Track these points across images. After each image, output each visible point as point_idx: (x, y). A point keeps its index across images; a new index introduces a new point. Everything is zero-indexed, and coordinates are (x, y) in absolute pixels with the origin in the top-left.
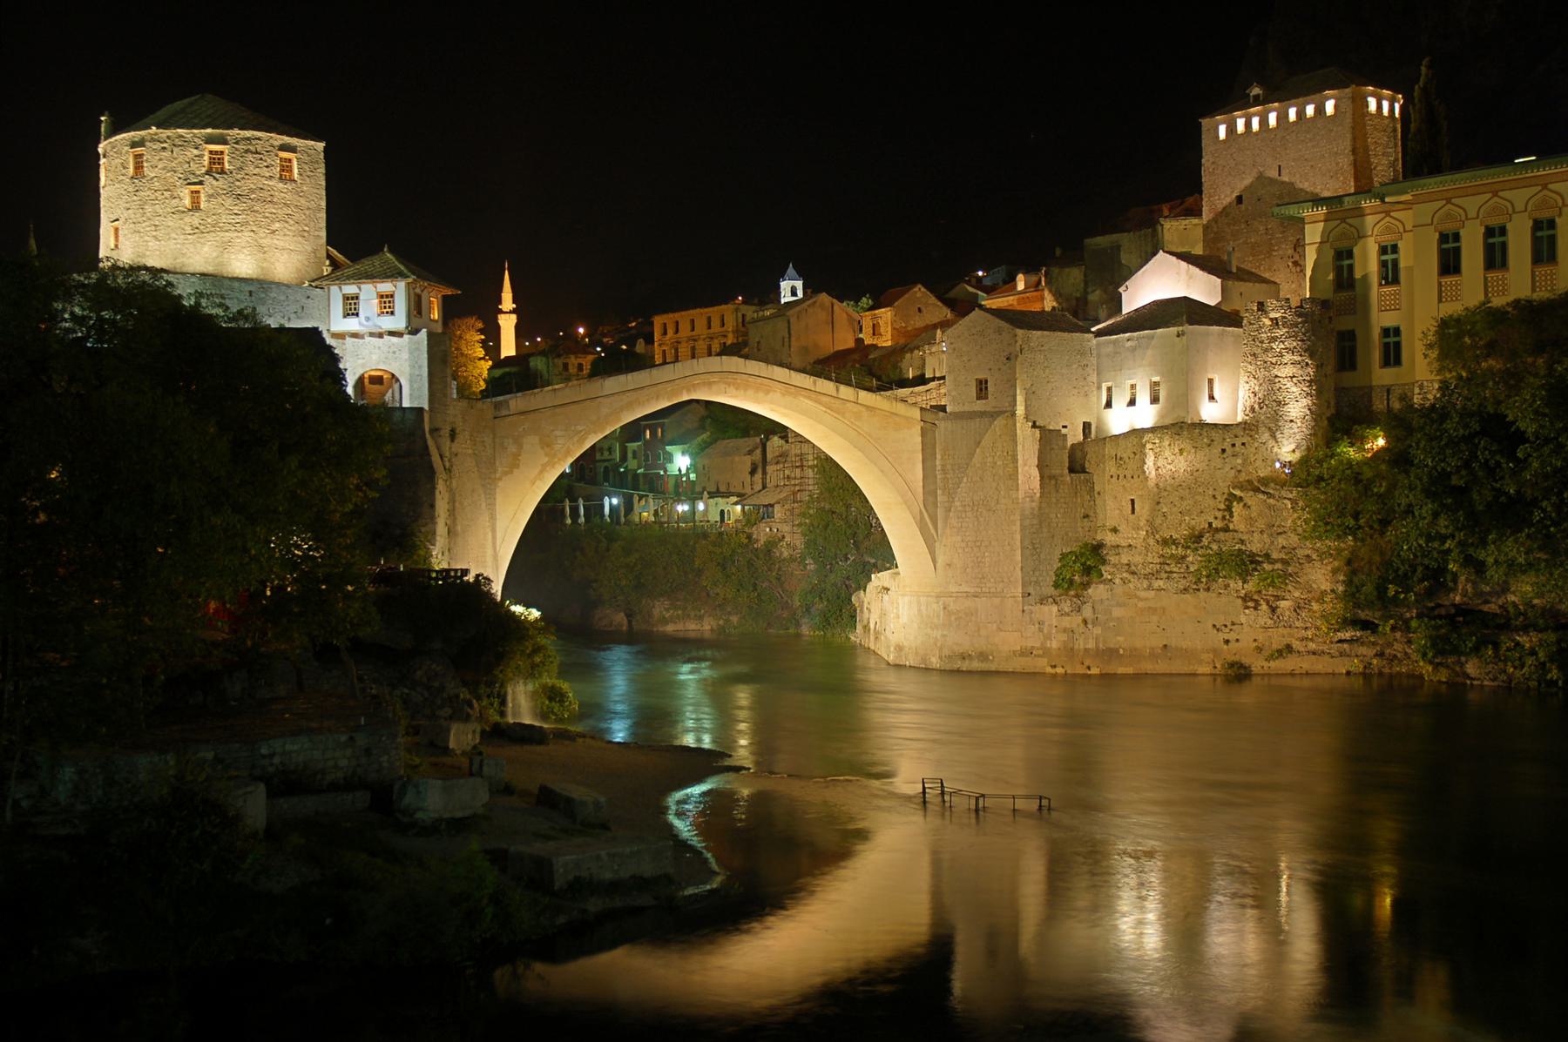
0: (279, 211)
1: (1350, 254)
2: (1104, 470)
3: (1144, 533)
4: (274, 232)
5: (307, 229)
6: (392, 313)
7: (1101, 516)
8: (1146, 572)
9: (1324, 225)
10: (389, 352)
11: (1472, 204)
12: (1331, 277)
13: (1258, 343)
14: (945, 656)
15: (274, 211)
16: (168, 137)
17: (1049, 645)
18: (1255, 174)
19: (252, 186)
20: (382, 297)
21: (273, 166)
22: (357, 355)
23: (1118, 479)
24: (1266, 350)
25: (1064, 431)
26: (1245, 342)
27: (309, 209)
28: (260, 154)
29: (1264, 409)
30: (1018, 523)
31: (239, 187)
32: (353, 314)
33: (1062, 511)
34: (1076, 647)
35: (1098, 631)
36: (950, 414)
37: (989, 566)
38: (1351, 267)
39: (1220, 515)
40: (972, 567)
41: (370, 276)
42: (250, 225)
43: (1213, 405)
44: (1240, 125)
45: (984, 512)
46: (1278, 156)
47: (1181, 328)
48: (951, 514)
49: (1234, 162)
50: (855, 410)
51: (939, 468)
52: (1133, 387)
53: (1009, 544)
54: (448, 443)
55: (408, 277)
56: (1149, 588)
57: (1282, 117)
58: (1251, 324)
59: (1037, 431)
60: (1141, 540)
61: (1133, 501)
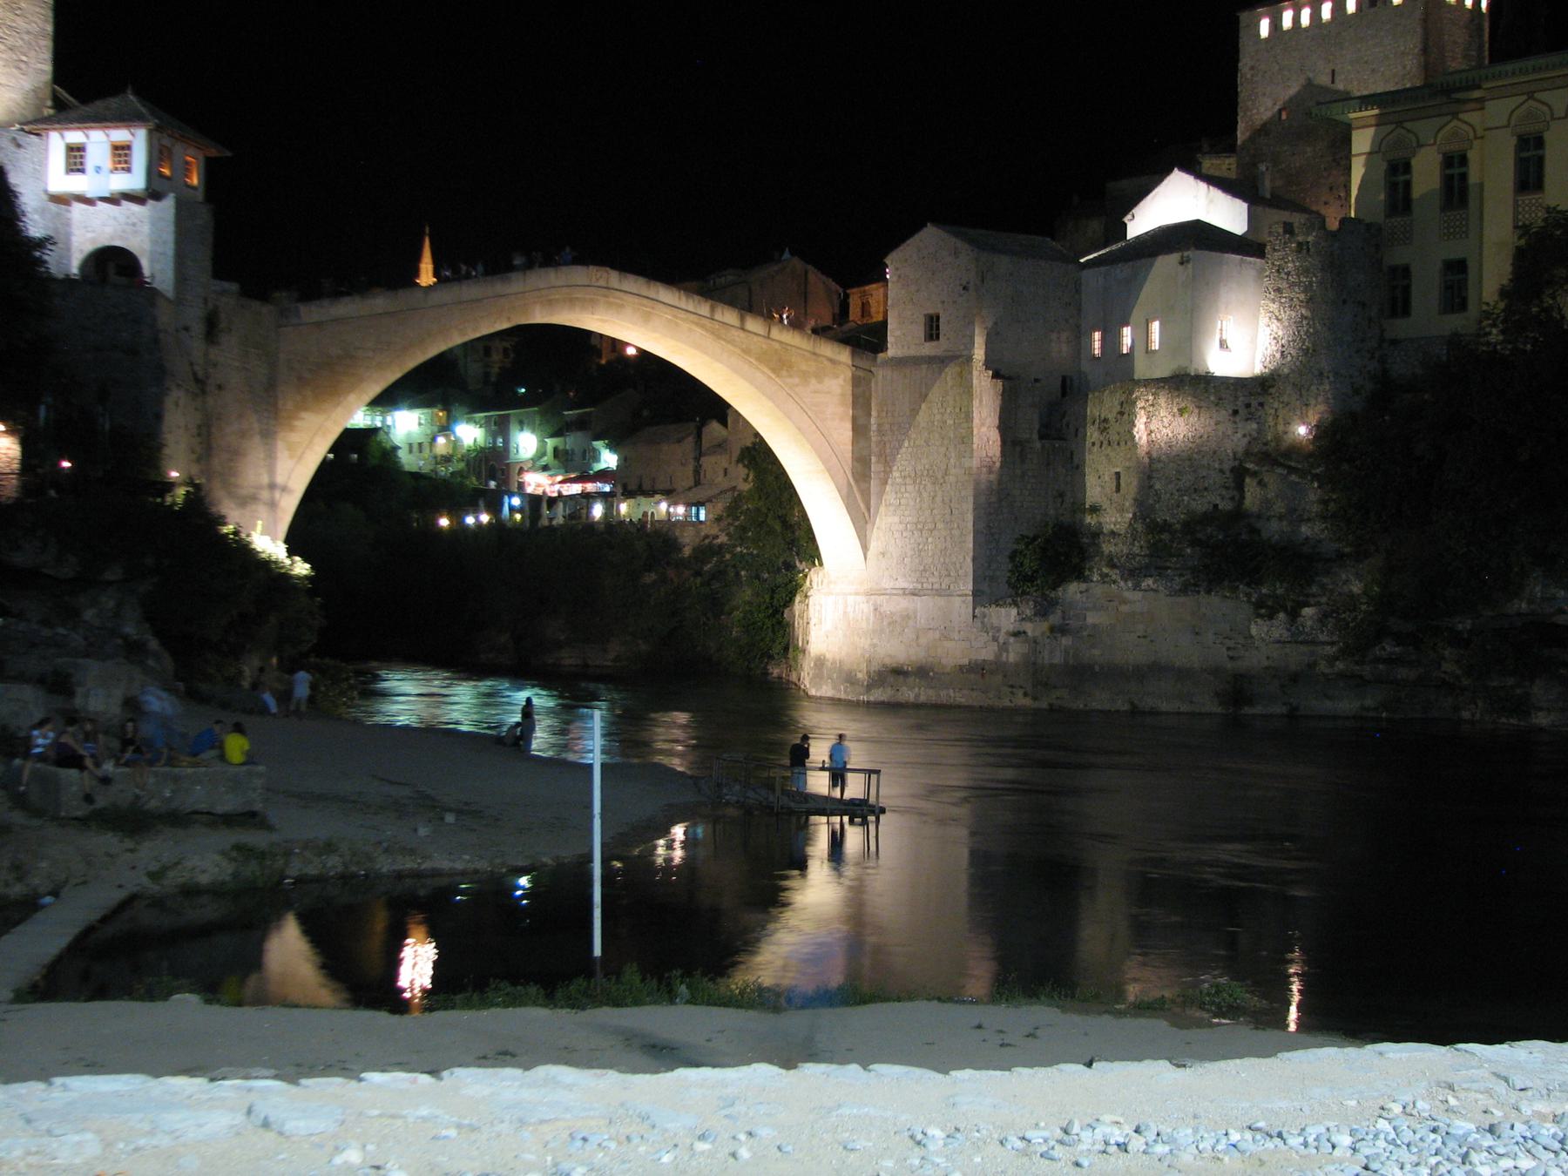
1: (1407, 168)
3: (1131, 515)
5: (24, 58)
9: (1376, 130)
12: (1382, 197)
13: (1283, 275)
14: (874, 671)
18: (1302, 81)
23: (1101, 447)
26: (1267, 273)
27: (28, 33)
30: (971, 499)
32: (79, 170)
33: (1029, 487)
34: (1039, 661)
35: (1066, 641)
37: (933, 555)
38: (1408, 184)
40: (912, 556)
43: (1224, 353)
45: (929, 485)
46: (1331, 57)
48: (888, 488)
49: (1277, 67)
51: (874, 427)
53: (958, 527)
56: (1137, 587)
58: (1275, 250)
61: (1118, 474)
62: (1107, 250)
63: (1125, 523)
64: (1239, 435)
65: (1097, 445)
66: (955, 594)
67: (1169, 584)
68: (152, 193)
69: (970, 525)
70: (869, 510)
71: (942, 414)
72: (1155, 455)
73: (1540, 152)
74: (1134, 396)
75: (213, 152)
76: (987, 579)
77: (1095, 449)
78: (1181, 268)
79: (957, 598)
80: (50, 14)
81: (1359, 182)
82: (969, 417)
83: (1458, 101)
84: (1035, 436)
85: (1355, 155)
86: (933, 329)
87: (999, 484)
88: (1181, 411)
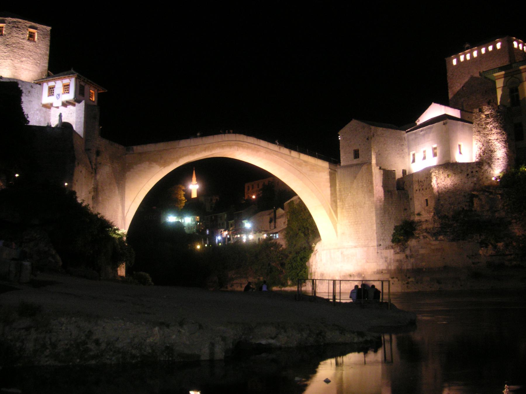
0: (26, 53)
1: (517, 90)
2: (413, 189)
3: (433, 214)
4: (22, 62)
5: (39, 62)
6: (69, 93)
7: (412, 209)
8: (434, 232)
10: (69, 114)
12: (509, 101)
14: (342, 276)
15: (23, 53)
18: (469, 76)
19: (14, 41)
21: (25, 34)
22: (55, 116)
23: (420, 191)
24: (484, 129)
26: (474, 126)
27: (40, 54)
28: (19, 28)
29: (485, 155)
31: (8, 41)
32: (52, 95)
36: (343, 166)
38: (518, 96)
39: (467, 204)
42: (10, 57)
43: (460, 155)
47: (445, 121)
50: (298, 162)
52: (424, 152)
54: (95, 157)
55: (75, 74)
57: (479, 53)
58: (476, 118)
59: (382, 171)
60: (431, 217)
61: (427, 200)
62: (414, 127)
63: (431, 216)
64: (470, 183)
65: (418, 191)
66: (370, 246)
67: (448, 238)
68: (77, 100)
69: (374, 221)
72: (440, 191)
74: (431, 171)
76: (382, 240)
77: (418, 191)
78: (444, 126)
79: (371, 247)
80: (49, 48)
82: (371, 183)
84: (395, 189)
85: (498, 88)
86: (356, 155)
87: (384, 206)
88: (448, 176)
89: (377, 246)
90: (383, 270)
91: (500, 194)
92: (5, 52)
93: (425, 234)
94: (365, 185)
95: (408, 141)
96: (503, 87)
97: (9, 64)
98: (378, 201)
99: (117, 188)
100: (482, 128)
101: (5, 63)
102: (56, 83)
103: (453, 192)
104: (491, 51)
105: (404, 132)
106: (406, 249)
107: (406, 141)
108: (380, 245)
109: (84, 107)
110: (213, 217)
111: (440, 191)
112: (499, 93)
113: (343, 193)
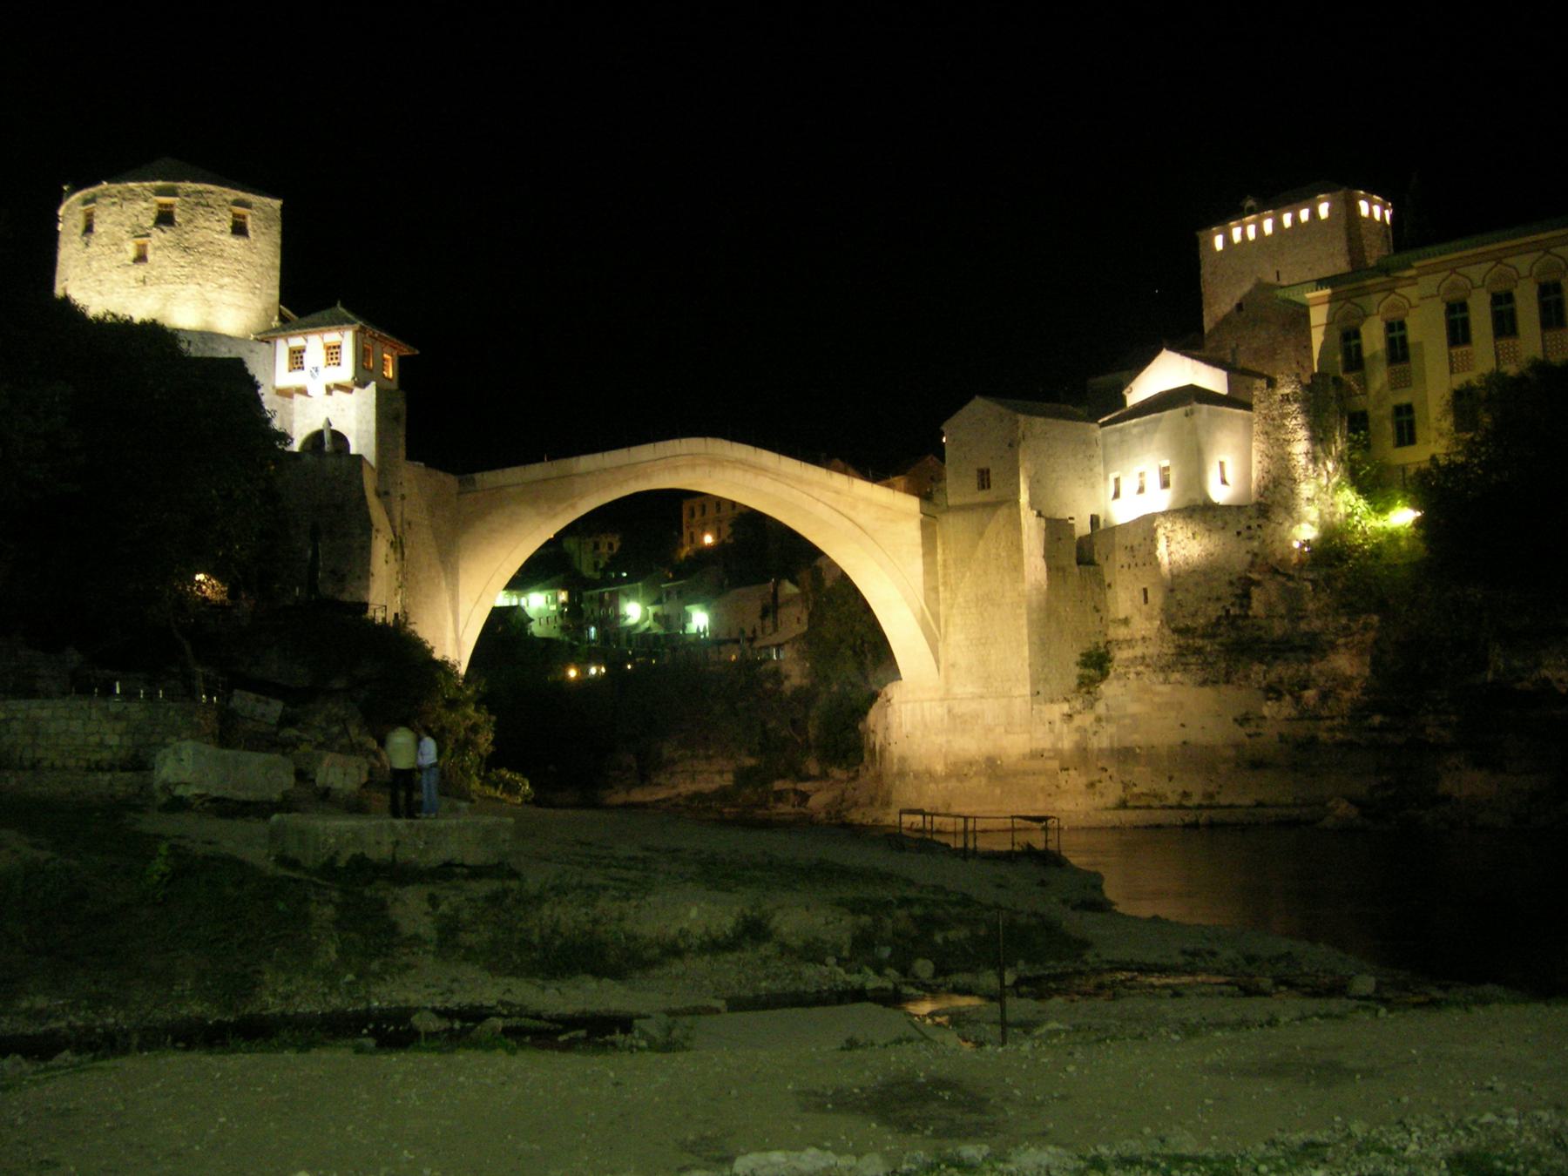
1: (1357, 335)
2: (1115, 560)
3: (1159, 622)
4: (221, 287)
5: (258, 286)
6: (339, 364)
11: (1477, 272)
12: (1339, 358)
13: (1269, 421)
15: (223, 265)
16: (119, 192)
17: (1060, 746)
18: (1253, 280)
20: (329, 348)
25: (1070, 522)
27: (261, 266)
30: (1025, 616)
31: (186, 239)
38: (1359, 348)
41: (316, 326)
44: (1236, 235)
47: (1188, 408)
52: (1141, 475)
56: (1166, 681)
57: (1278, 224)
59: (1043, 521)
61: (1145, 591)
64: (1243, 551)
65: (1126, 568)
69: (1025, 638)
70: (939, 631)
71: (997, 549)
73: (1465, 314)
75: (406, 351)
80: (279, 251)
81: (1319, 345)
82: (1019, 549)
83: (1398, 279)
84: (1074, 562)
89: (1032, 695)
90: (1043, 750)
91: (1311, 581)
92: (182, 267)
93: (1140, 668)
94: (1003, 554)
95: (1105, 446)
96: (1327, 325)
97: (193, 295)
98: (1034, 592)
99: (442, 574)
100: (1274, 425)
101: (183, 293)
102: (306, 340)
103: (1205, 573)
104: (1306, 223)
105: (1094, 426)
106: (1097, 704)
107: (1100, 446)
108: (1038, 693)
109: (374, 396)
110: (606, 595)
111: (1175, 571)
112: (1317, 338)
113: (952, 571)
